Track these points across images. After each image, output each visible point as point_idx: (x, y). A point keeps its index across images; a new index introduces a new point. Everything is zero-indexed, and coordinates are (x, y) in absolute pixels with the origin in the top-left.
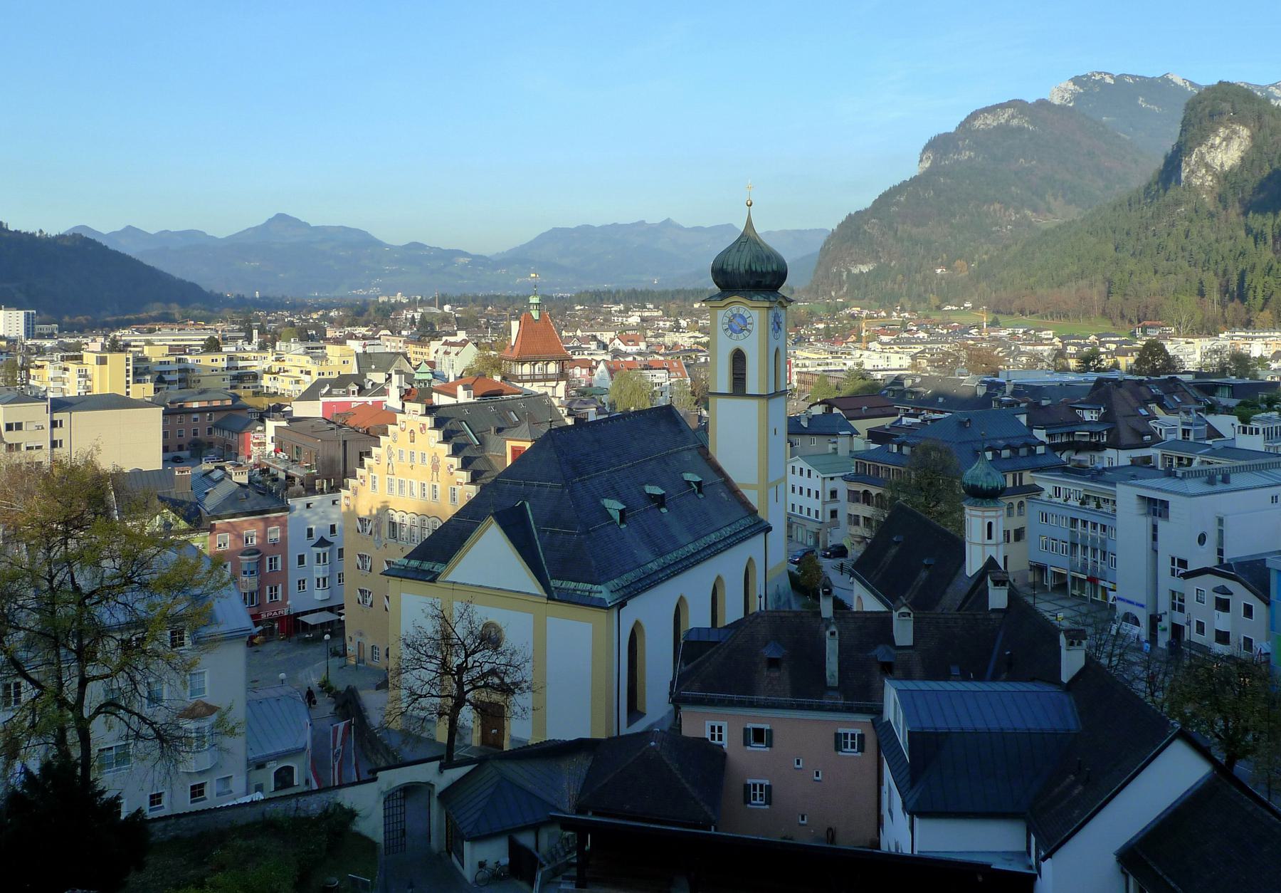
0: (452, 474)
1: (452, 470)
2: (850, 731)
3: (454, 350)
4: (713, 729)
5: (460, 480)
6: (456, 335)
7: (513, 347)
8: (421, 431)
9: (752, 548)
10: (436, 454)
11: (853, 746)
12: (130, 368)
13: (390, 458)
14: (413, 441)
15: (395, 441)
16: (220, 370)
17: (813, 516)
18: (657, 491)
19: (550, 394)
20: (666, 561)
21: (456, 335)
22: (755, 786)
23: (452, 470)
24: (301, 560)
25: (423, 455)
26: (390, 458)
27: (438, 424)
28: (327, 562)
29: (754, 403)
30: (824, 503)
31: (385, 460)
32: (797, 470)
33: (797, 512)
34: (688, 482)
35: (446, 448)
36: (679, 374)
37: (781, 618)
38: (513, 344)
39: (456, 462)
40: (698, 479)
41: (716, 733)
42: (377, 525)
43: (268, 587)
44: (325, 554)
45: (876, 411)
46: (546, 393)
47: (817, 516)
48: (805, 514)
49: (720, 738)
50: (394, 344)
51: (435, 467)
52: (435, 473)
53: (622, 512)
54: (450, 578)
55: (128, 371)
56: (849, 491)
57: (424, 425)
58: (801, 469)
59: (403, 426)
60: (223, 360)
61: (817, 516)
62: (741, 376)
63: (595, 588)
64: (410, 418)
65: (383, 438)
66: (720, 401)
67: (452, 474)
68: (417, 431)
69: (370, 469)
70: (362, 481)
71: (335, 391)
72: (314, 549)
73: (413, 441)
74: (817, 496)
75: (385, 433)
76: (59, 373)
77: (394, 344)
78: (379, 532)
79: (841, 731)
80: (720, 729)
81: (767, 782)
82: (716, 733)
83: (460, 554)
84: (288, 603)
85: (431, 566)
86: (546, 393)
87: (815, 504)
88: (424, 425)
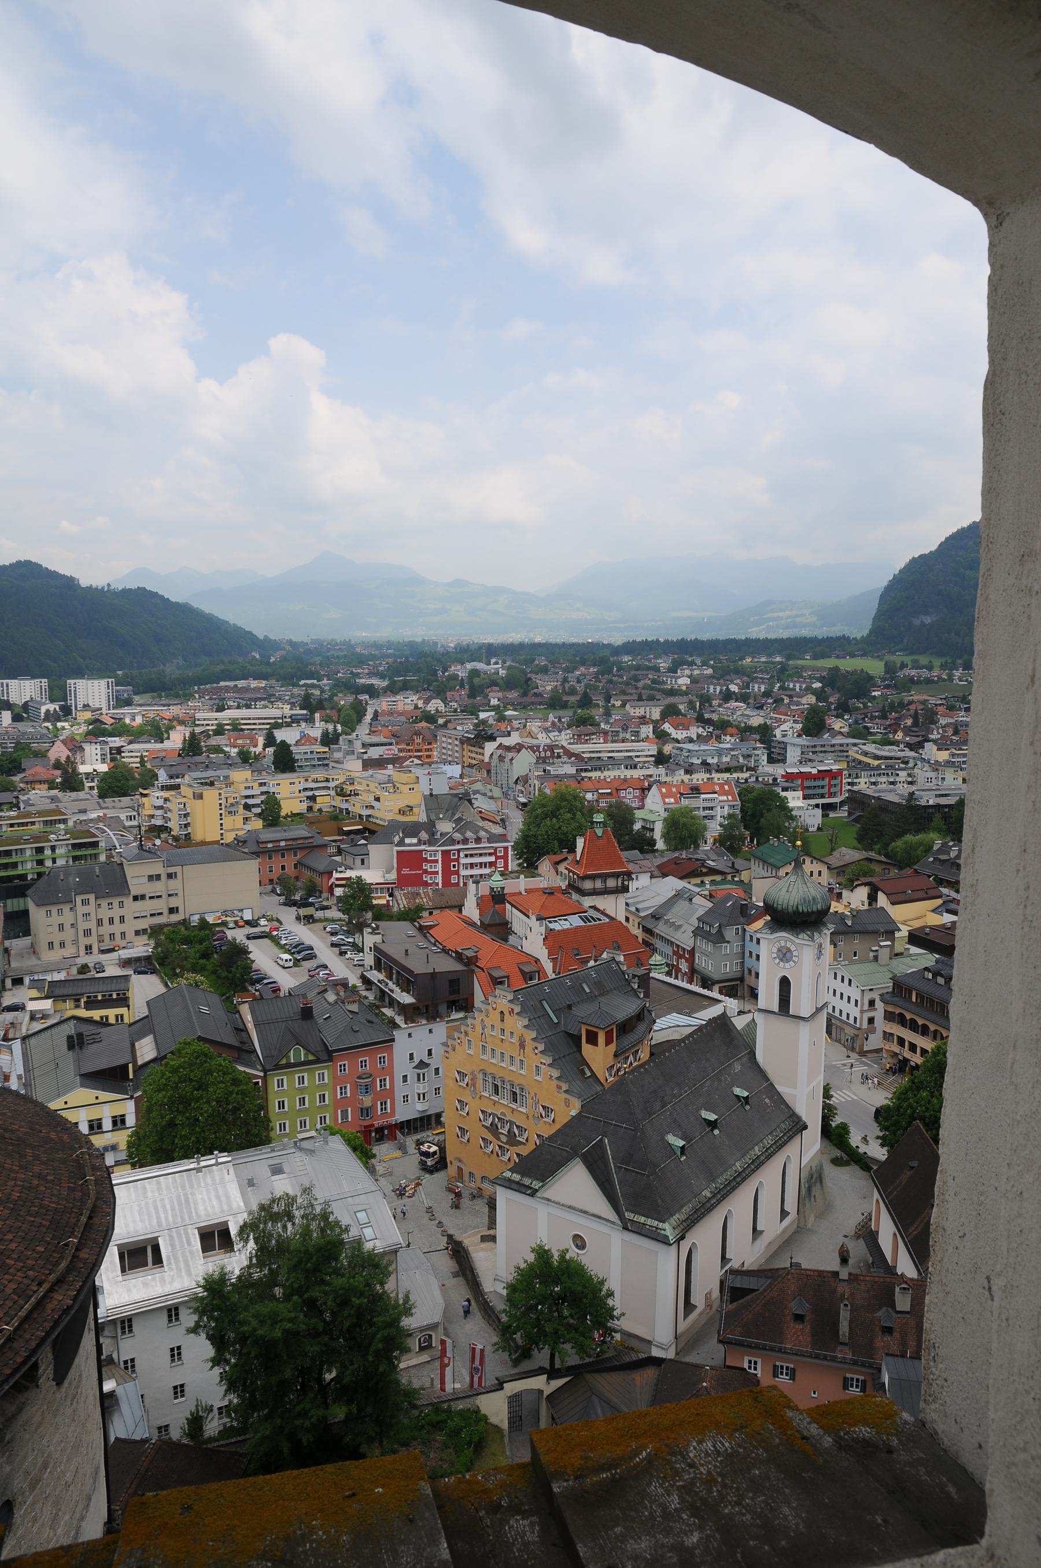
0: (536, 1054)
2: (855, 1377)
3: (510, 755)
4: (750, 1362)
6: (509, 735)
9: (791, 1150)
11: (857, 1386)
14: (502, 1020)
17: (851, 1021)
18: (712, 1117)
20: (718, 1185)
21: (509, 735)
22: (782, 1367)
23: (536, 1051)
26: (483, 1029)
30: (862, 1012)
32: (839, 978)
33: (837, 1014)
34: (737, 1096)
36: (730, 798)
37: (807, 1275)
40: (746, 1094)
41: (753, 1365)
42: (472, 1079)
45: (921, 894)
47: (855, 1022)
48: (844, 1017)
49: (755, 1369)
50: (450, 741)
51: (522, 1046)
53: (683, 1148)
54: (545, 1195)
56: (885, 1011)
57: (512, 1010)
58: (843, 977)
59: (494, 1006)
61: (855, 1022)
63: (661, 1225)
68: (506, 1013)
71: (407, 841)
73: (502, 1020)
74: (856, 1005)
77: (450, 741)
78: (474, 1085)
79: (848, 1375)
80: (755, 1363)
81: (792, 1366)
82: (753, 1365)
85: (530, 1181)
87: (855, 1012)
88: (512, 1010)
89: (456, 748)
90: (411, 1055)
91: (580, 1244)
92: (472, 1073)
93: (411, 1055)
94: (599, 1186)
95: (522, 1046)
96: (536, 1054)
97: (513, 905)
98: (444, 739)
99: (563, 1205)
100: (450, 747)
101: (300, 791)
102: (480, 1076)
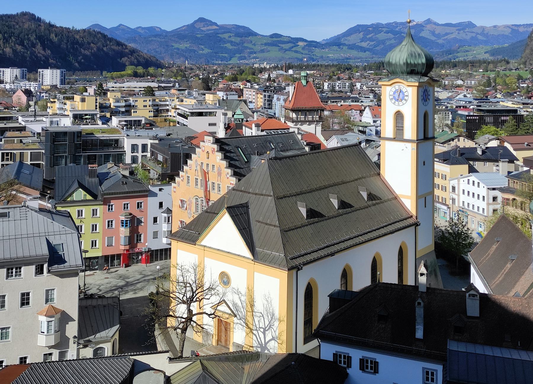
1: (228, 176)
5: (232, 182)
7: (290, 101)
8: (212, 152)
10: (220, 166)
12: (98, 104)
13: (196, 167)
15: (199, 157)
16: (148, 106)
19: (296, 132)
24: (155, 220)
25: (213, 166)
26: (196, 167)
27: (221, 149)
28: (170, 222)
29: (409, 145)
31: (194, 168)
35: (224, 163)
38: (290, 100)
39: (229, 171)
43: (135, 235)
44: (169, 218)
46: (294, 132)
50: (250, 93)
51: (220, 174)
52: (219, 177)
54: (203, 243)
55: (96, 106)
57: (214, 149)
59: (203, 149)
60: (150, 101)
62: (401, 128)
64: (207, 145)
65: (193, 155)
66: (387, 142)
67: (228, 178)
68: (210, 152)
69: (187, 172)
70: (182, 178)
72: (163, 214)
75: (195, 153)
76: (62, 106)
77: (250, 93)
78: (190, 209)
83: (208, 230)
84: (146, 244)
86: (294, 132)
88: (214, 149)
89: (254, 97)
90: (161, 205)
91: (225, 280)
92: (189, 200)
93: (161, 205)
94: (239, 230)
95: (220, 174)
96: (228, 178)
97: (246, 126)
98: (247, 93)
99: (214, 249)
100: (250, 96)
101: (150, 106)
102: (194, 201)
